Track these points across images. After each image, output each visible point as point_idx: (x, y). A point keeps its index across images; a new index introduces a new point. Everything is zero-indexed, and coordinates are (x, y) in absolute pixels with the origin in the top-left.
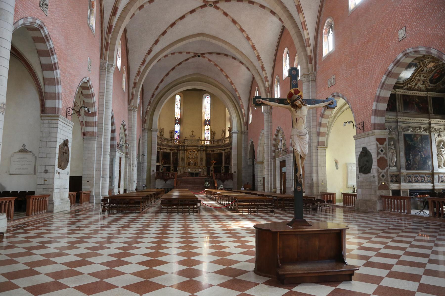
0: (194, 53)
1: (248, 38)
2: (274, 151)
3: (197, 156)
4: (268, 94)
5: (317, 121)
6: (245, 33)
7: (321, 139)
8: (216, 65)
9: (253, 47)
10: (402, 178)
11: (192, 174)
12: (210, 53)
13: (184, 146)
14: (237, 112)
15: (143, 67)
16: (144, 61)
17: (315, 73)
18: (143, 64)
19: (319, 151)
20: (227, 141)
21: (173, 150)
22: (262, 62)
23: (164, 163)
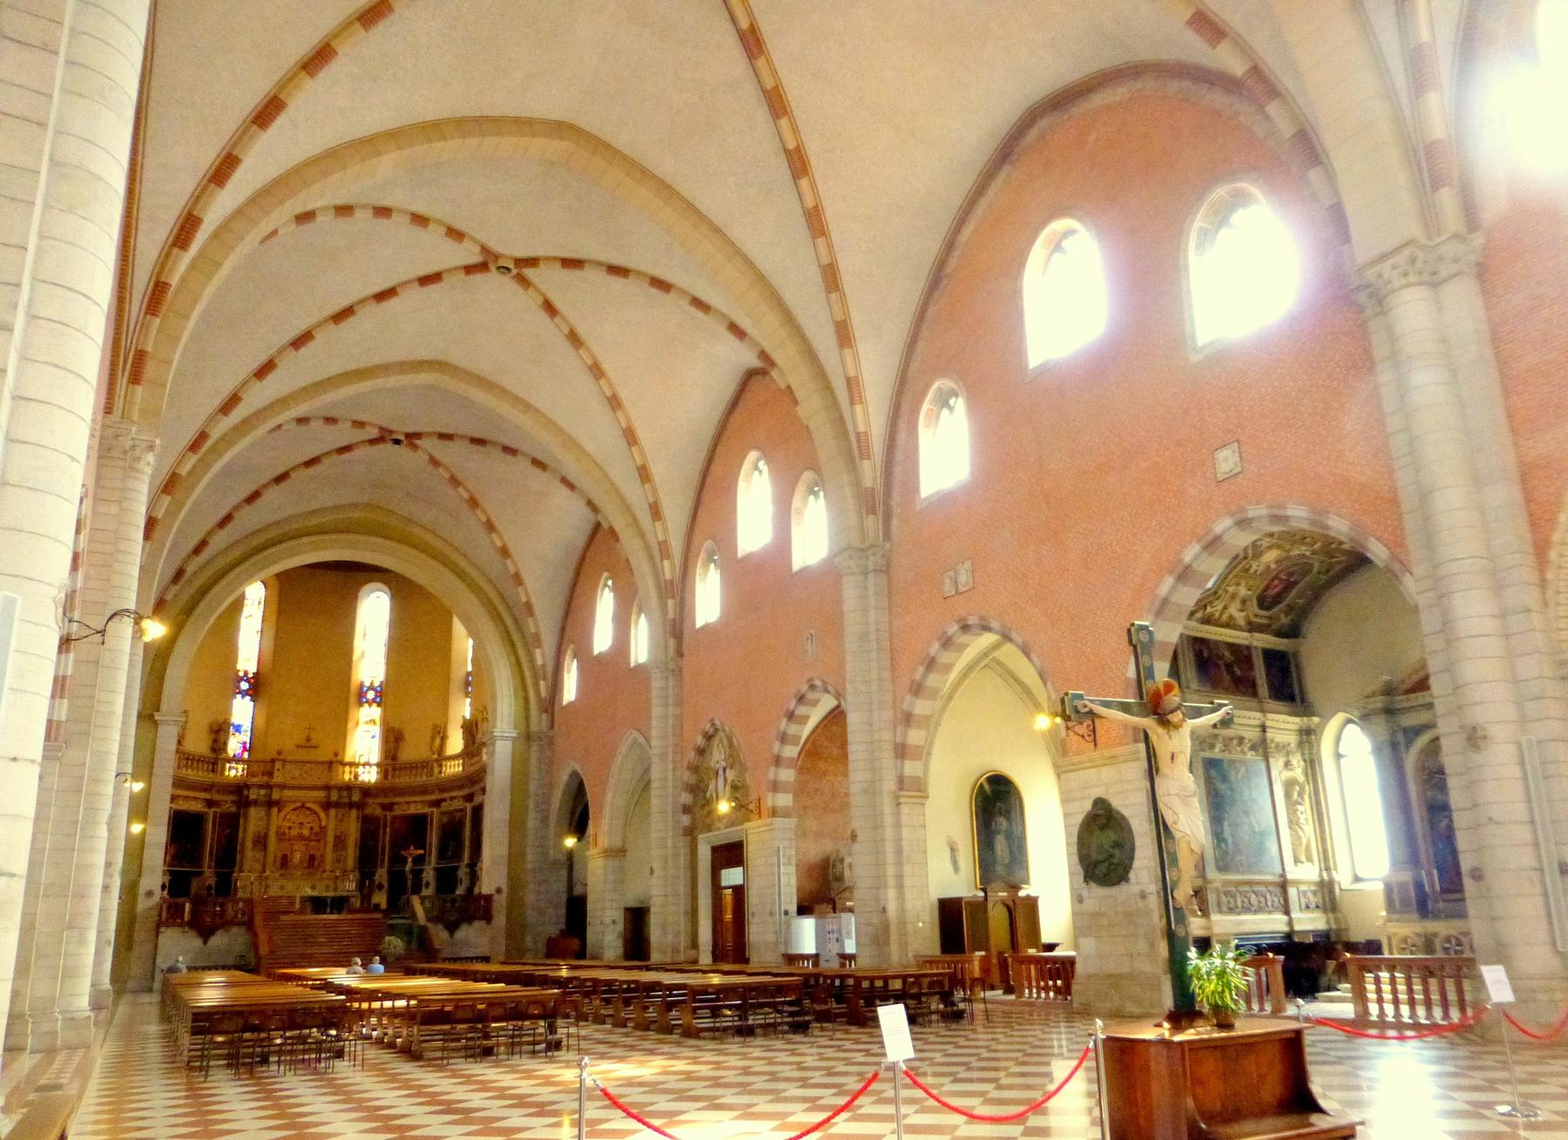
0: (382, 429)
1: (614, 402)
2: (687, 810)
3: (323, 829)
4: (670, 602)
5: (894, 708)
6: (609, 381)
7: (911, 768)
8: (455, 481)
9: (630, 436)
10: (1212, 898)
11: (318, 904)
12: (444, 436)
13: (269, 787)
14: (513, 659)
15: (193, 459)
16: (203, 436)
17: (888, 545)
18: (194, 447)
19: (905, 809)
20: (454, 768)
22: (654, 490)
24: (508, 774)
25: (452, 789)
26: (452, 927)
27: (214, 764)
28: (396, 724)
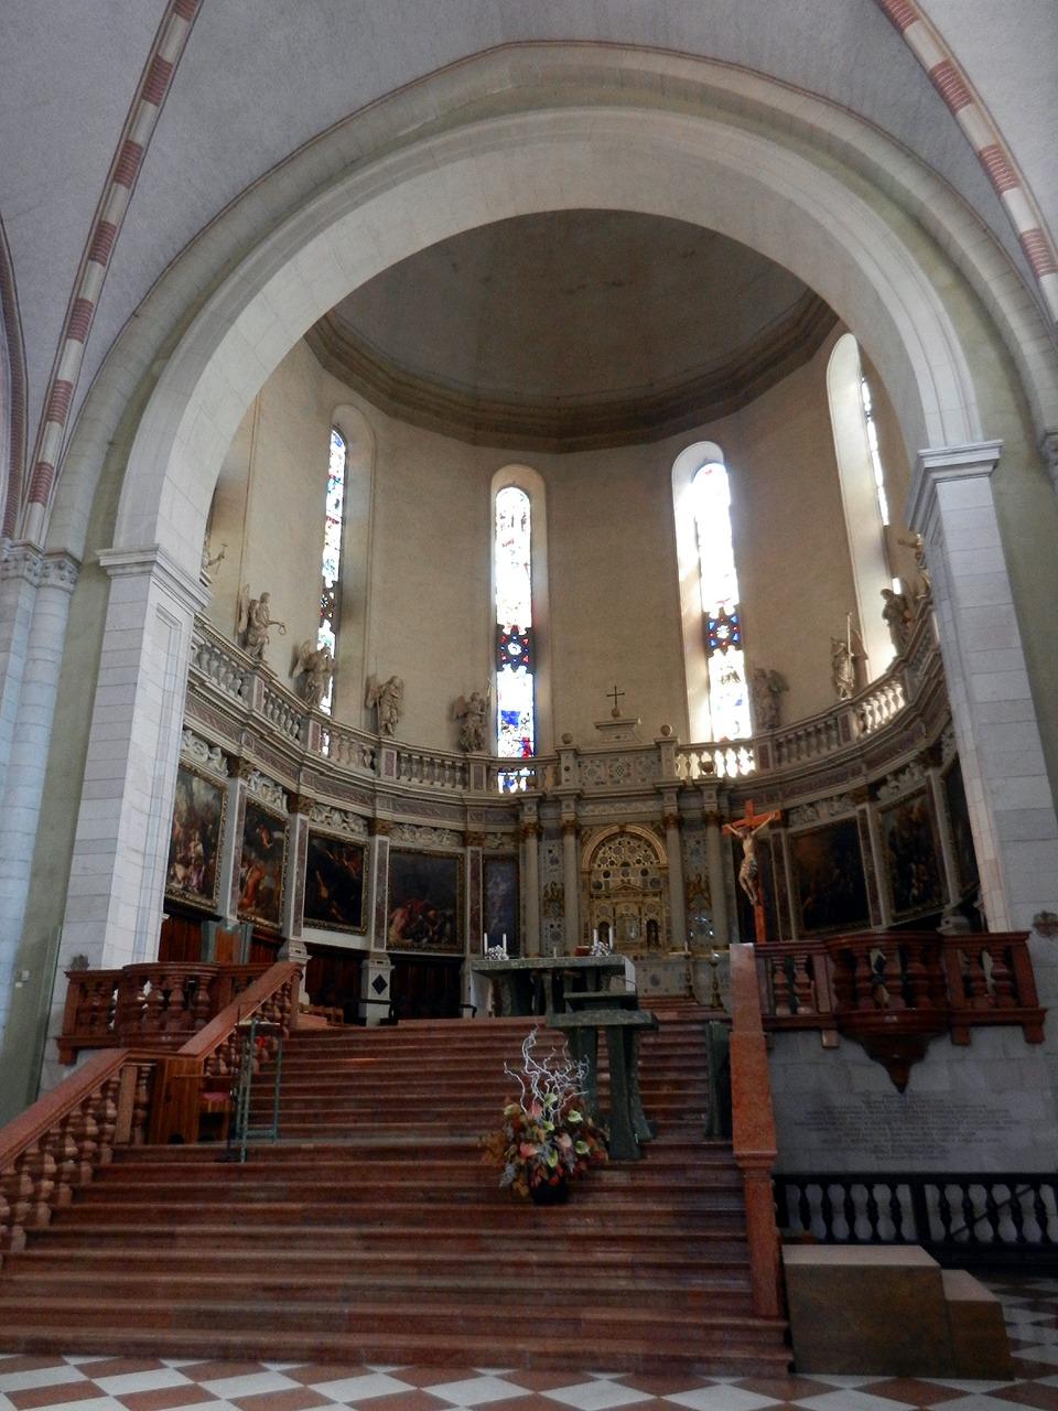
14: (945, 277)
21: (478, 839)
23: (404, 932)
24: (998, 563)
25: (891, 753)
26: (898, 1053)
27: (464, 770)
28: (767, 667)
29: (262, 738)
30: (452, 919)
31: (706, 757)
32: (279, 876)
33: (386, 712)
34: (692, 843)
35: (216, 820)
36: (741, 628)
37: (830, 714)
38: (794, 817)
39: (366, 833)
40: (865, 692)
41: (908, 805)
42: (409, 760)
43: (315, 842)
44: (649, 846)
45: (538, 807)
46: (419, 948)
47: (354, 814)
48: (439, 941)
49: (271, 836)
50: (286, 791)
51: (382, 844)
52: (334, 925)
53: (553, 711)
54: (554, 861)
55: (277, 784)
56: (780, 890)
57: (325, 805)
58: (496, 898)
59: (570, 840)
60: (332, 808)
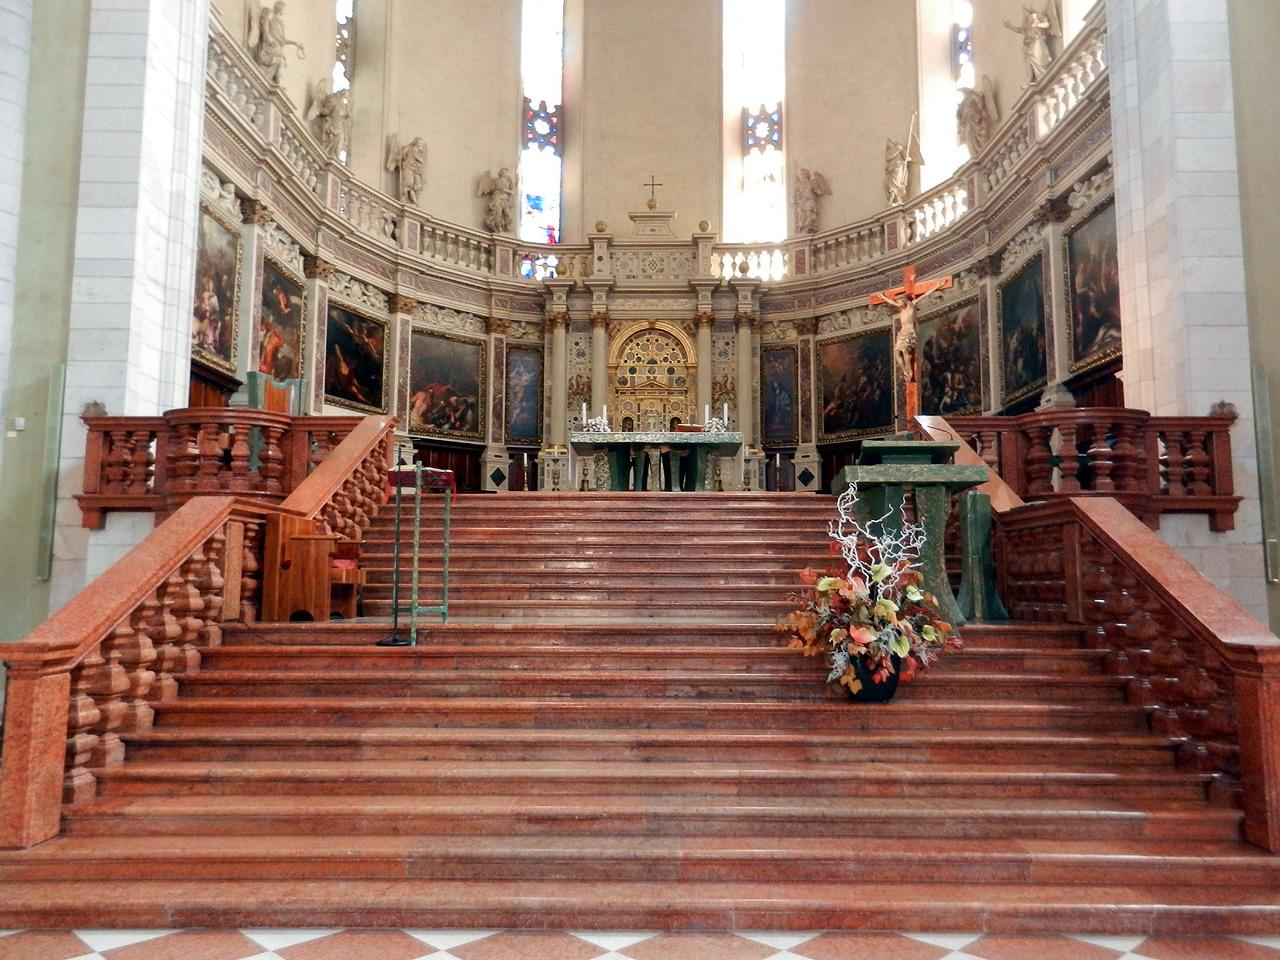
21: (502, 326)
29: (279, 182)
30: (473, 407)
31: (740, 258)
32: (297, 344)
33: (408, 176)
34: (721, 345)
35: (231, 271)
36: (781, 127)
37: (878, 220)
38: (823, 325)
39: (386, 310)
40: (914, 201)
41: (952, 316)
42: (433, 234)
43: (334, 314)
44: (677, 345)
45: (568, 297)
46: (441, 433)
47: (375, 287)
48: (460, 428)
49: (288, 299)
50: (303, 252)
51: (405, 323)
52: (355, 404)
53: (583, 199)
54: (581, 354)
55: (294, 242)
56: (804, 393)
57: (345, 274)
58: (517, 389)
59: (600, 333)
60: (353, 278)
